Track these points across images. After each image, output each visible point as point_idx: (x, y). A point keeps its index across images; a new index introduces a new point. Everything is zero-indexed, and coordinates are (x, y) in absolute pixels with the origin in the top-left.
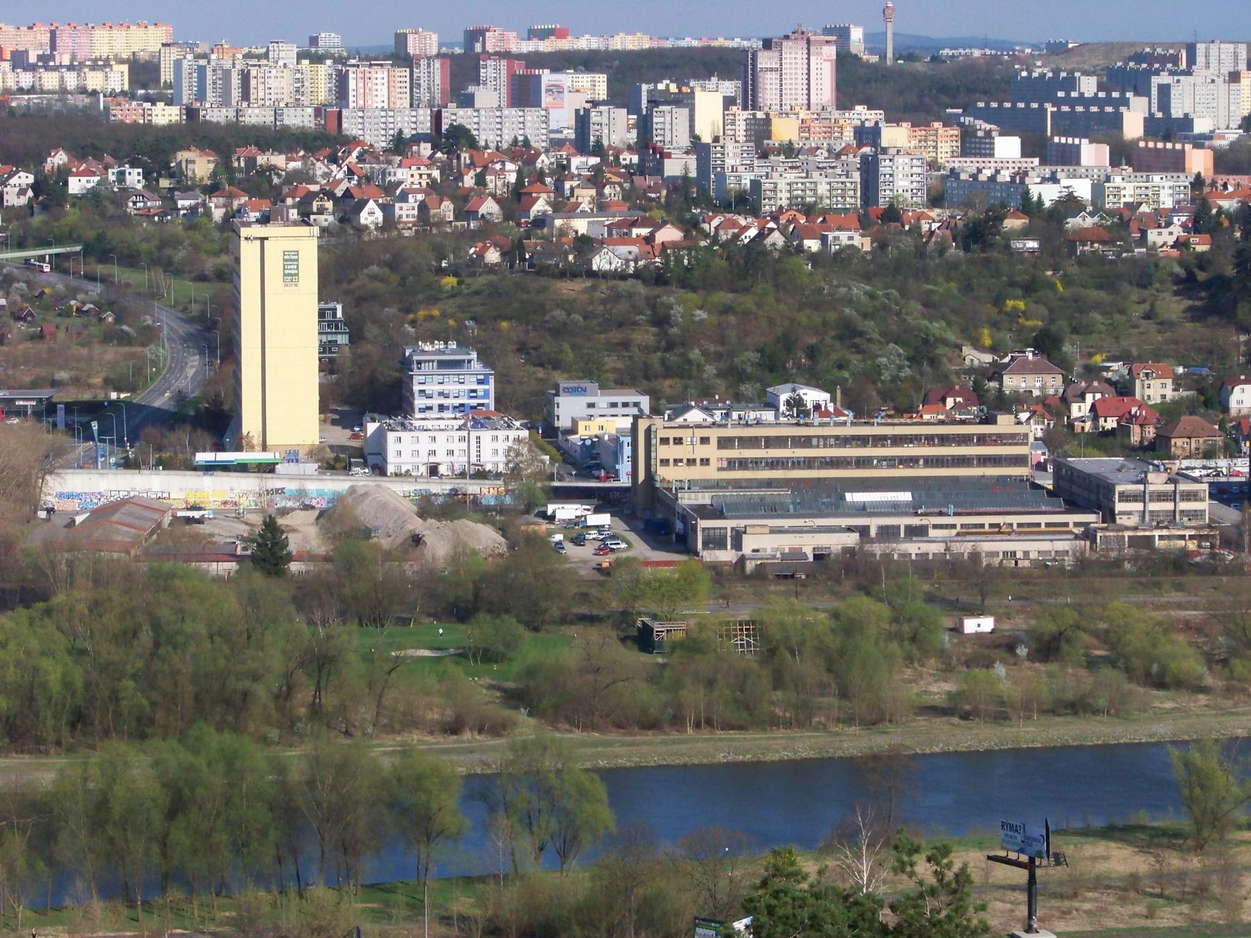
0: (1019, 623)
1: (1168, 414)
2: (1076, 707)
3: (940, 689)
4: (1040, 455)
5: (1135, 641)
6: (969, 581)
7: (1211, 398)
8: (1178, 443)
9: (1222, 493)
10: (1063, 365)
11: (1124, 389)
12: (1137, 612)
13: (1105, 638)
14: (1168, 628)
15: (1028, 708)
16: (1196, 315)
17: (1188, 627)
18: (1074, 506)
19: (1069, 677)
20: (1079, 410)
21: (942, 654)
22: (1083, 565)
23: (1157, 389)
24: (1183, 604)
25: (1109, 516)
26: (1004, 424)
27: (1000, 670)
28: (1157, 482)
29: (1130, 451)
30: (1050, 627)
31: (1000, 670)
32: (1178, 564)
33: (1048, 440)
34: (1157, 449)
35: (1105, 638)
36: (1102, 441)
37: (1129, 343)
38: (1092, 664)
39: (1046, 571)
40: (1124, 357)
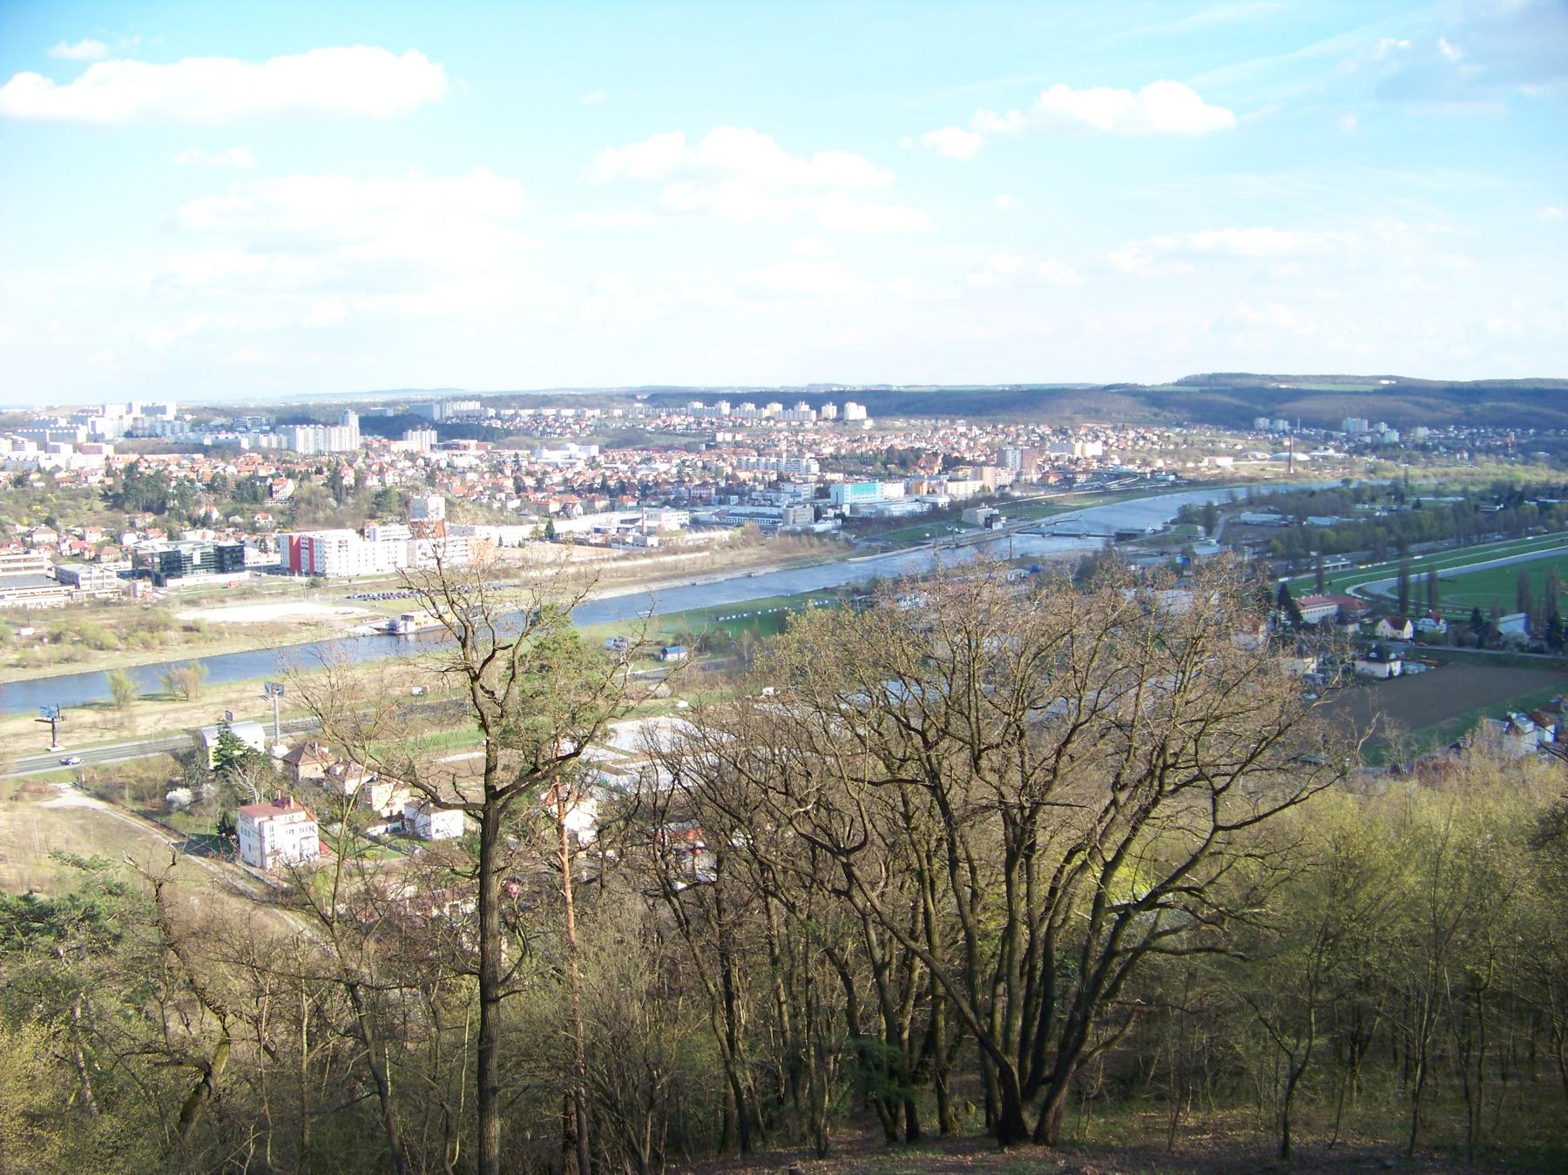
0: (44, 630)
1: (100, 546)
2: (68, 660)
3: (14, 658)
4: (49, 564)
5: (90, 633)
6: (24, 615)
7: (116, 539)
8: (104, 558)
9: (122, 575)
10: (57, 530)
11: (82, 538)
12: (91, 622)
13: (78, 633)
14: (103, 627)
15: (49, 662)
16: (109, 508)
17: (111, 626)
18: (63, 583)
19: (65, 649)
20: (64, 547)
21: (14, 644)
22: (68, 606)
23: (95, 537)
24: (107, 617)
25: (78, 586)
26: (34, 553)
27: (37, 648)
28: (96, 572)
29: (85, 561)
30: (56, 631)
31: (37, 648)
32: (106, 603)
33: (53, 559)
34: (96, 559)
35: (78, 633)
36: (75, 557)
37: (83, 520)
38: (74, 643)
39: (54, 609)
40: (81, 526)
